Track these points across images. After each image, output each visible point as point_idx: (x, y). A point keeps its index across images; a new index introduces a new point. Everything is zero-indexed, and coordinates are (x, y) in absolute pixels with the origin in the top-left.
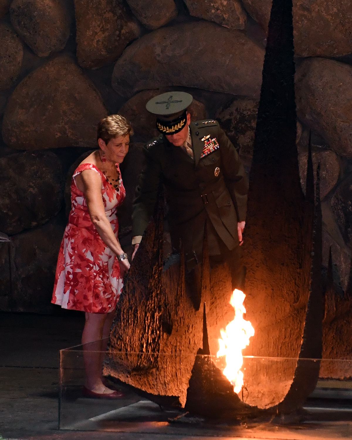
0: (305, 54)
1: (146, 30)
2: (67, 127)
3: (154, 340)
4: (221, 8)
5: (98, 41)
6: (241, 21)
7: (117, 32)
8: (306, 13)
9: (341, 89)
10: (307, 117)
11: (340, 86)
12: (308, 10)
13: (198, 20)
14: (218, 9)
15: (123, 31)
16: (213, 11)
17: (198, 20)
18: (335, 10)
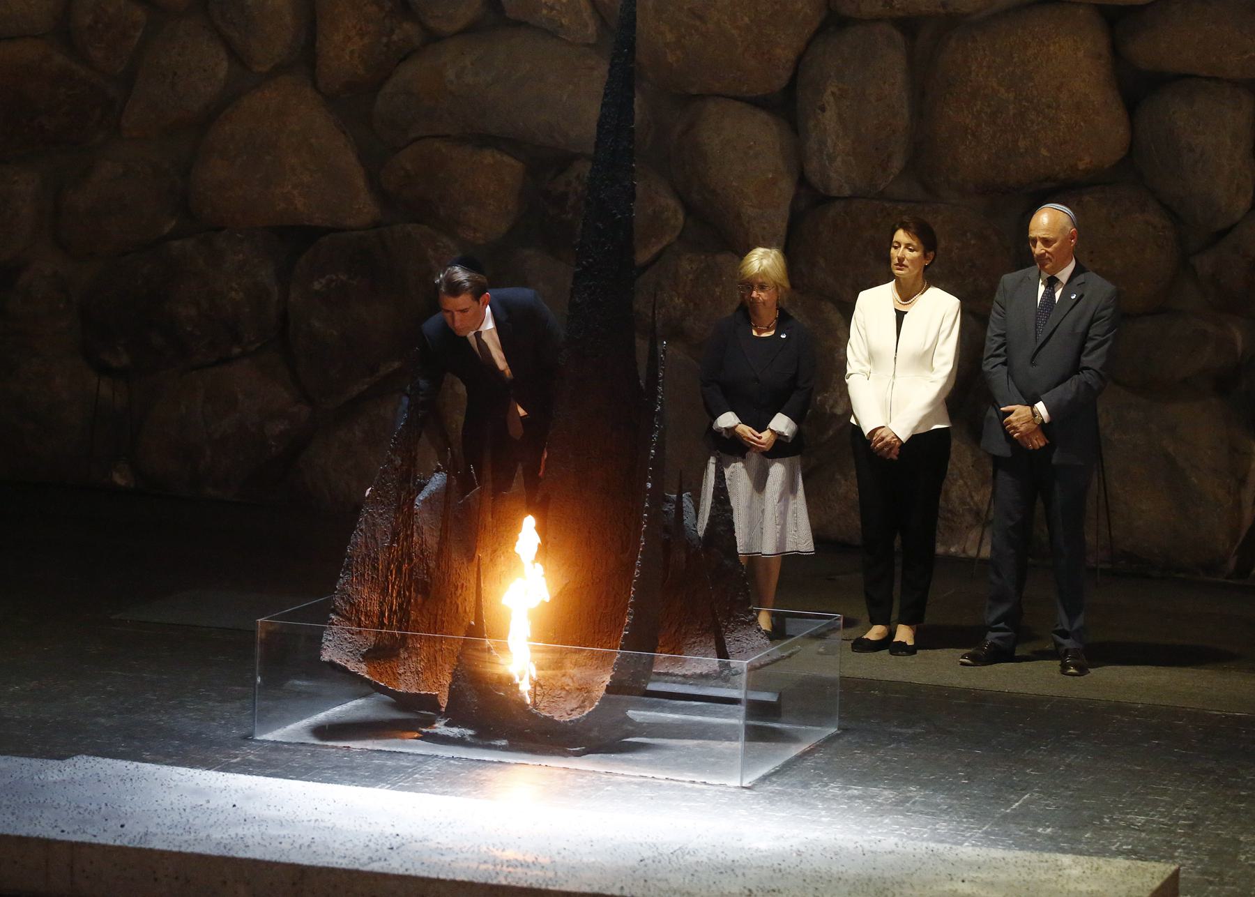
0: (694, 91)
1: (433, 38)
2: (295, 192)
3: (400, 606)
4: (558, 7)
5: (352, 52)
6: (592, 29)
7: (385, 40)
8: (698, 23)
9: (751, 152)
11: (750, 147)
12: (701, 18)
13: (518, 24)
14: (552, 8)
15: (395, 37)
16: (545, 12)
17: (518, 24)
18: (746, 19)
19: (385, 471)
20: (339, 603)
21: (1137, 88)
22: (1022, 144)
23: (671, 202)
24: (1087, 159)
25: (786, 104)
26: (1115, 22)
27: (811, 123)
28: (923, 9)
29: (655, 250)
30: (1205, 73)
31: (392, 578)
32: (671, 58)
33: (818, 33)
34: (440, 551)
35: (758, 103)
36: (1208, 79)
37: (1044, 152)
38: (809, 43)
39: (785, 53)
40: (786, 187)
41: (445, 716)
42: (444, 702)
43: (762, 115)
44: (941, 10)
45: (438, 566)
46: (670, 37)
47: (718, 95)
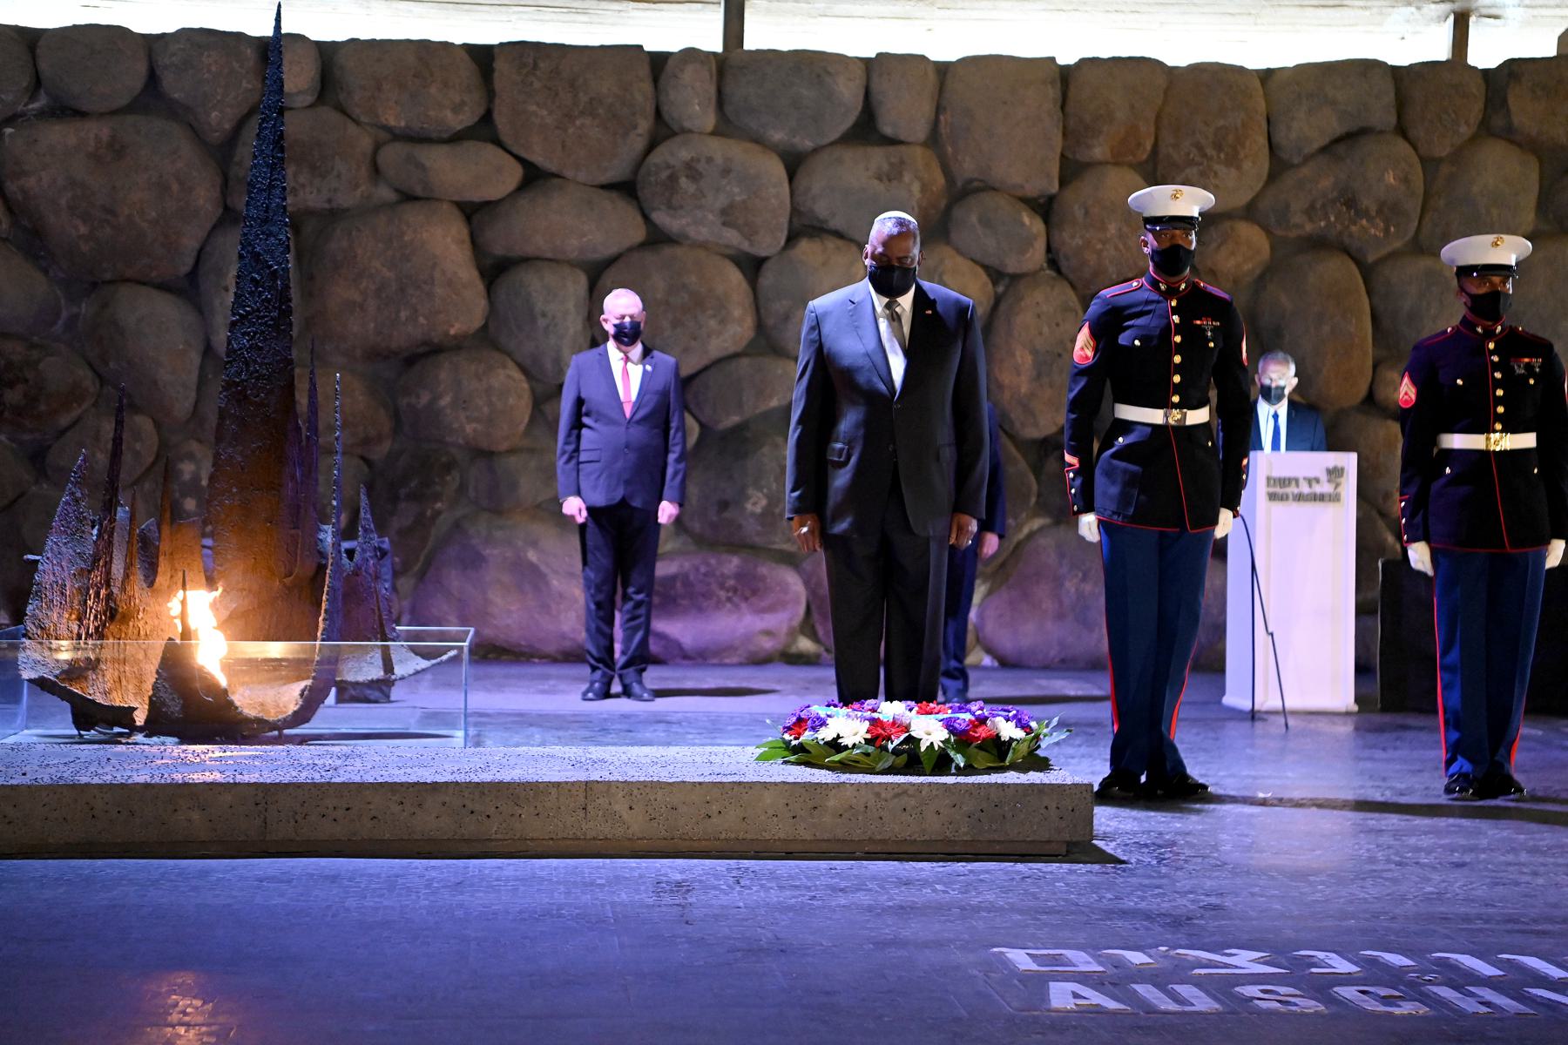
0: (108, 276)
3: (97, 628)
10: (112, 365)
19: (67, 503)
20: (30, 626)
21: (495, 270)
22: (403, 315)
23: (90, 374)
24: (457, 326)
25: (188, 288)
26: (473, 213)
27: (217, 302)
28: (311, 204)
29: (75, 413)
30: (549, 255)
31: (90, 603)
32: (84, 248)
33: (214, 227)
34: (127, 576)
35: (164, 287)
36: (550, 260)
37: (421, 320)
38: (210, 235)
39: (190, 242)
40: (195, 358)
41: (140, 729)
42: (140, 718)
43: (168, 296)
44: (327, 206)
45: (123, 589)
46: (83, 230)
47: (128, 280)
